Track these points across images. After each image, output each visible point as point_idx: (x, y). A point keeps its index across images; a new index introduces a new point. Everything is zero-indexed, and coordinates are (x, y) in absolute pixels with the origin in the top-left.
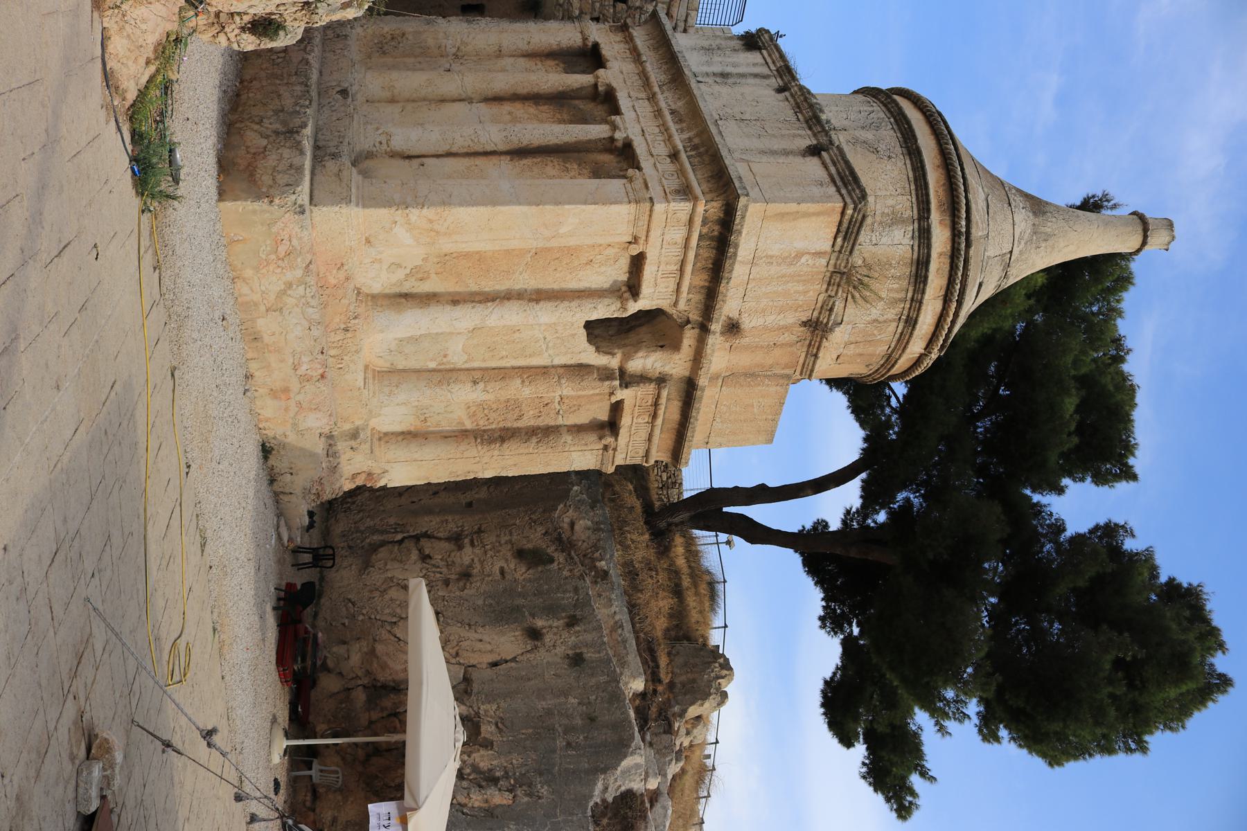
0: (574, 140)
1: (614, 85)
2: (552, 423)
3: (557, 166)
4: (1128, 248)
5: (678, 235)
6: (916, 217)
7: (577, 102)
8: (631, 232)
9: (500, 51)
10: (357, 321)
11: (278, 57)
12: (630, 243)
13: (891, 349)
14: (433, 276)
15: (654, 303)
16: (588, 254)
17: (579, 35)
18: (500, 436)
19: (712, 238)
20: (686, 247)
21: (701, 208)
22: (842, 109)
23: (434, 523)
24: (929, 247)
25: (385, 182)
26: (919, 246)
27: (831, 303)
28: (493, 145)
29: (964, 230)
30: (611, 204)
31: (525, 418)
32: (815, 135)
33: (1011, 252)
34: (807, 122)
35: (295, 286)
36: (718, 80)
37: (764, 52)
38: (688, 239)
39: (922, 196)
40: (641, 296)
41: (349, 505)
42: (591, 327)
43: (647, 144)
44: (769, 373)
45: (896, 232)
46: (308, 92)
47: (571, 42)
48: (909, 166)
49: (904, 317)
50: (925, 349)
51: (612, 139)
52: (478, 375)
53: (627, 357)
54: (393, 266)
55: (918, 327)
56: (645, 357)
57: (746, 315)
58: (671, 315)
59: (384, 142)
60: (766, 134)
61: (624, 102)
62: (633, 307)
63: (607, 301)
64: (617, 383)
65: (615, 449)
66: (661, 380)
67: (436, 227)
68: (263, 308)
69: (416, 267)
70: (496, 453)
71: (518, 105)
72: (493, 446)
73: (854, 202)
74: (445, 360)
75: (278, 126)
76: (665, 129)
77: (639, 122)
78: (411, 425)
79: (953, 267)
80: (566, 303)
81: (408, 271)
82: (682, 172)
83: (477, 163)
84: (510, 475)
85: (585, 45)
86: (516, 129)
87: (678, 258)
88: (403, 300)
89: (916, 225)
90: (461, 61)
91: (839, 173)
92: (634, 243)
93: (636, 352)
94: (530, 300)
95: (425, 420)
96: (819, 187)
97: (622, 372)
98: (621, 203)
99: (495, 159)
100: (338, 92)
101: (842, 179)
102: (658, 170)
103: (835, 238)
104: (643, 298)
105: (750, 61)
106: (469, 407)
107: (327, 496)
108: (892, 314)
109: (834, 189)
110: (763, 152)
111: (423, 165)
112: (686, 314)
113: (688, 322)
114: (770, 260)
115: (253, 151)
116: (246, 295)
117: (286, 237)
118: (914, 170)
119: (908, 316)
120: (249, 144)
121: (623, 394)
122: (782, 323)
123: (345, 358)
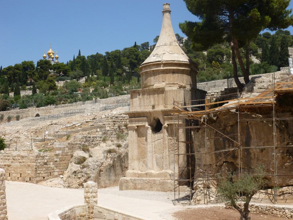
14: (144, 159)
68: (135, 186)
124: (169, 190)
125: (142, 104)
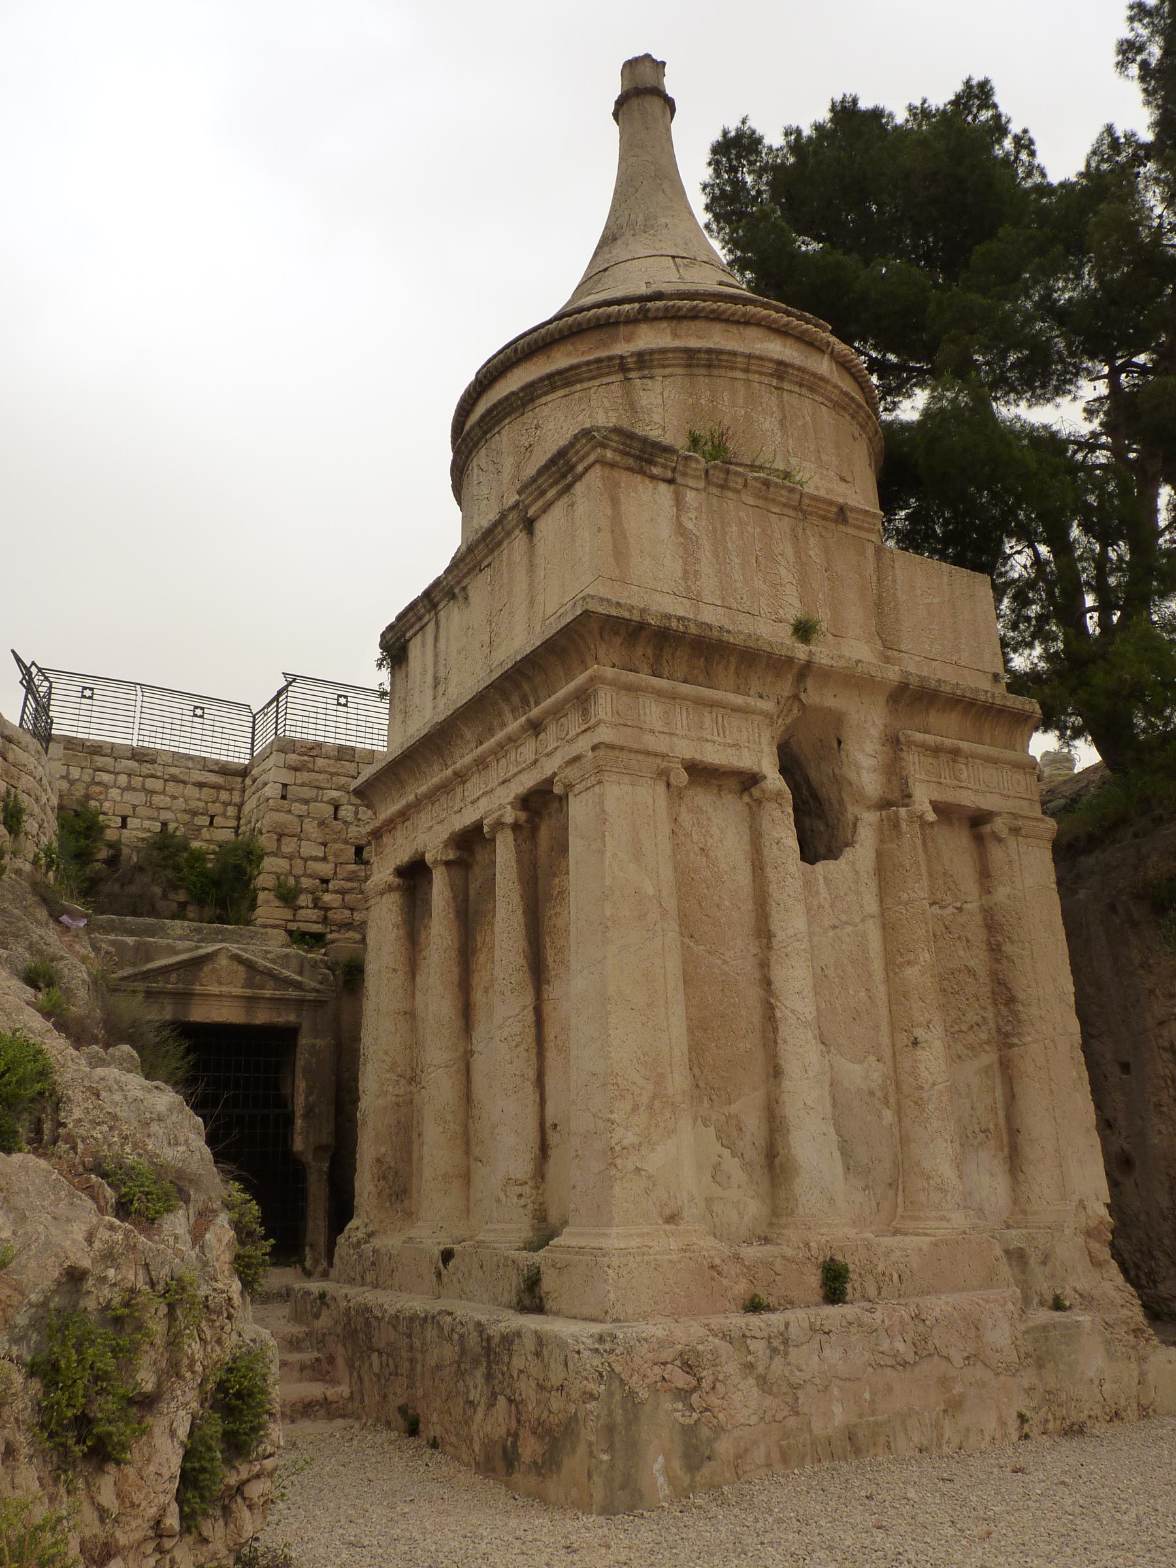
0: (517, 886)
1: (445, 836)
2: (978, 919)
3: (557, 909)
4: (664, 114)
5: (652, 712)
6: (620, 377)
7: (472, 892)
8: (651, 782)
9: (405, 1013)
10: (813, 1244)
11: (387, 1365)
12: (668, 785)
13: (826, 402)
14: (734, 1108)
15: (766, 749)
16: (692, 854)
17: (385, 897)
18: (1006, 1005)
19: (658, 657)
20: (674, 697)
21: (609, 672)
22: (476, 508)
23: (1163, 1128)
24: (663, 351)
25: (574, 1187)
26: (664, 367)
27: (757, 484)
28: (526, 1012)
29: (637, 306)
30: (604, 811)
31: (971, 963)
32: (508, 534)
33: (673, 257)
34: (492, 551)
35: (750, 1358)
36: (441, 689)
37: (408, 635)
38: (659, 693)
39: (590, 371)
40: (756, 769)
41: (1141, 1274)
42: (809, 854)
43: (520, 772)
44: (874, 578)
45: (644, 402)
46: (433, 1317)
47: (395, 908)
48: (549, 398)
49: (774, 382)
50: (823, 352)
51: (516, 827)
52: (903, 1039)
53: (860, 797)
54: (718, 1178)
55: (787, 360)
56: (858, 768)
57: (781, 610)
58: (788, 728)
59: (518, 1190)
60: (508, 605)
61: (468, 818)
62: (774, 780)
63: (766, 825)
64: (903, 811)
65: (1015, 816)
66: (894, 743)
67: (645, 1099)
68: (792, 1422)
69: (719, 1138)
70: (1034, 1011)
71: (476, 979)
72: (1023, 1016)
73: (593, 448)
74: (879, 1094)
75: (479, 1373)
76: (500, 750)
77: (492, 790)
78: (994, 1156)
79: (694, 315)
80: (773, 888)
81: (726, 1153)
82: (557, 712)
83: (552, 1037)
84: (1072, 989)
85: (398, 888)
86: (502, 976)
87: (690, 710)
88: (777, 1161)
89: (632, 375)
90: (418, 1072)
91: (556, 482)
92: (668, 777)
93: (850, 784)
94: (769, 947)
95: (985, 1131)
96: (575, 507)
97: (885, 804)
98: (602, 796)
99: (547, 1008)
100: (445, 1266)
101: (564, 476)
102: (556, 749)
103: (653, 477)
104: (759, 764)
105: (419, 653)
106: (959, 1057)
107: (1137, 1314)
108: (770, 400)
109: (578, 485)
110: (532, 603)
111: (556, 1125)
112: (783, 701)
113: (796, 697)
114: (690, 573)
115: (514, 1424)
116: (768, 1455)
117: (657, 1369)
118: (554, 389)
119: (772, 375)
120: (503, 1430)
121: (922, 798)
122: (792, 559)
123: (881, 1268)
124: (1097, 1410)
125: (708, 584)
